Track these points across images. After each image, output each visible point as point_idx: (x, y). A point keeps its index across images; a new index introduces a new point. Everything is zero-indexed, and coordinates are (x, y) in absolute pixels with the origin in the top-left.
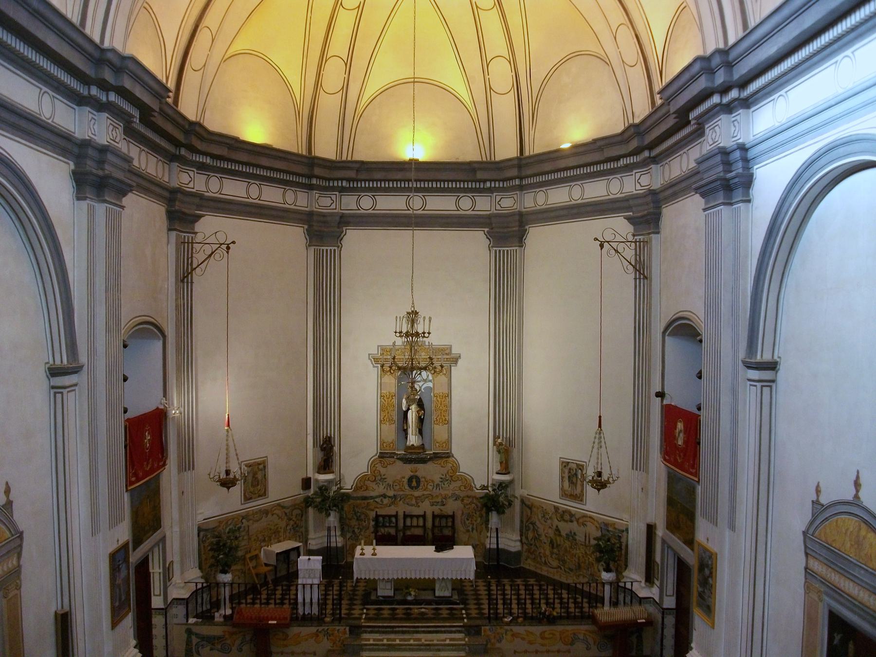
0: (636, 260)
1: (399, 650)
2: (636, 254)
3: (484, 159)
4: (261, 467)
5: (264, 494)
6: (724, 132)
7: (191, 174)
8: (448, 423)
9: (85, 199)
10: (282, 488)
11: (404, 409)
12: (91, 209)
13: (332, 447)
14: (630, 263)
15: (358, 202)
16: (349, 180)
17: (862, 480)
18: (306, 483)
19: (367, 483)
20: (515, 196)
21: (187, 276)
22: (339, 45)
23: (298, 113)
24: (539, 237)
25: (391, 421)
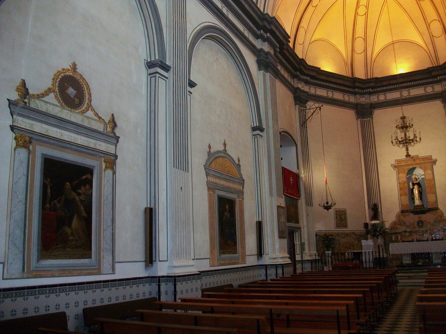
1: (414, 279)
3: (434, 66)
4: (344, 213)
5: (346, 226)
7: (303, 85)
8: (435, 193)
10: (354, 225)
11: (411, 187)
12: (264, 76)
13: (377, 209)
15: (378, 98)
16: (373, 88)
18: (366, 225)
19: (397, 226)
22: (360, 32)
23: (346, 64)
25: (405, 194)
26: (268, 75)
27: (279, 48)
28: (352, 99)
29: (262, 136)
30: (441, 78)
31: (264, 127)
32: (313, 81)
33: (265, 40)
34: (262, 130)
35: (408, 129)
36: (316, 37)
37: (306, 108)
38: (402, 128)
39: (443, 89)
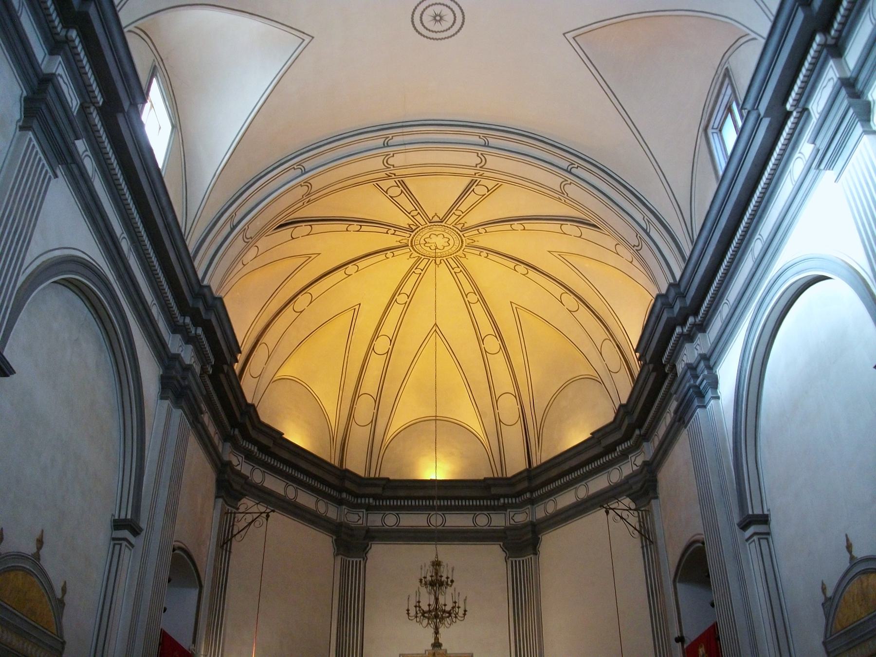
0: (640, 525)
2: (640, 521)
3: (496, 476)
6: (689, 354)
9: (166, 399)
14: (635, 529)
15: (383, 519)
16: (376, 497)
17: (851, 540)
20: (527, 511)
21: (227, 543)
22: (370, 385)
23: (332, 439)
24: (552, 543)
26: (178, 413)
27: (212, 366)
28: (332, 512)
29: (132, 546)
30: (506, 501)
31: (143, 525)
32: (264, 457)
33: (189, 339)
34: (136, 532)
35: (443, 588)
36: (287, 371)
37: (238, 509)
38: (432, 584)
39: (508, 524)
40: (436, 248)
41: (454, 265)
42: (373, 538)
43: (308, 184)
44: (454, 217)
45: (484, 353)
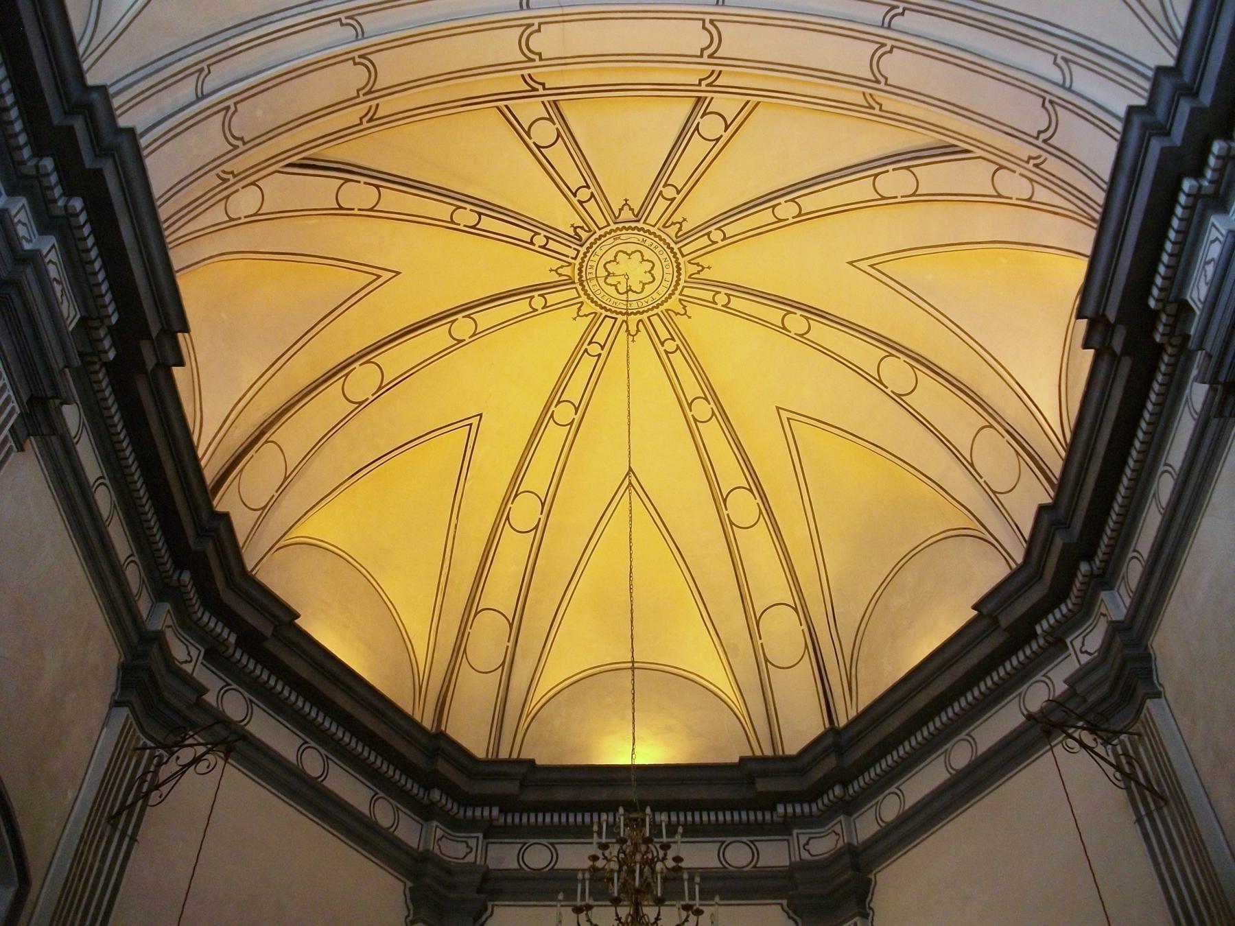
7: (194, 653)
15: (521, 855)
22: (501, 590)
27: (111, 329)
28: (408, 831)
40: (629, 290)
41: (664, 335)
42: (497, 894)
43: (364, 59)
44: (662, 204)
45: (728, 527)
